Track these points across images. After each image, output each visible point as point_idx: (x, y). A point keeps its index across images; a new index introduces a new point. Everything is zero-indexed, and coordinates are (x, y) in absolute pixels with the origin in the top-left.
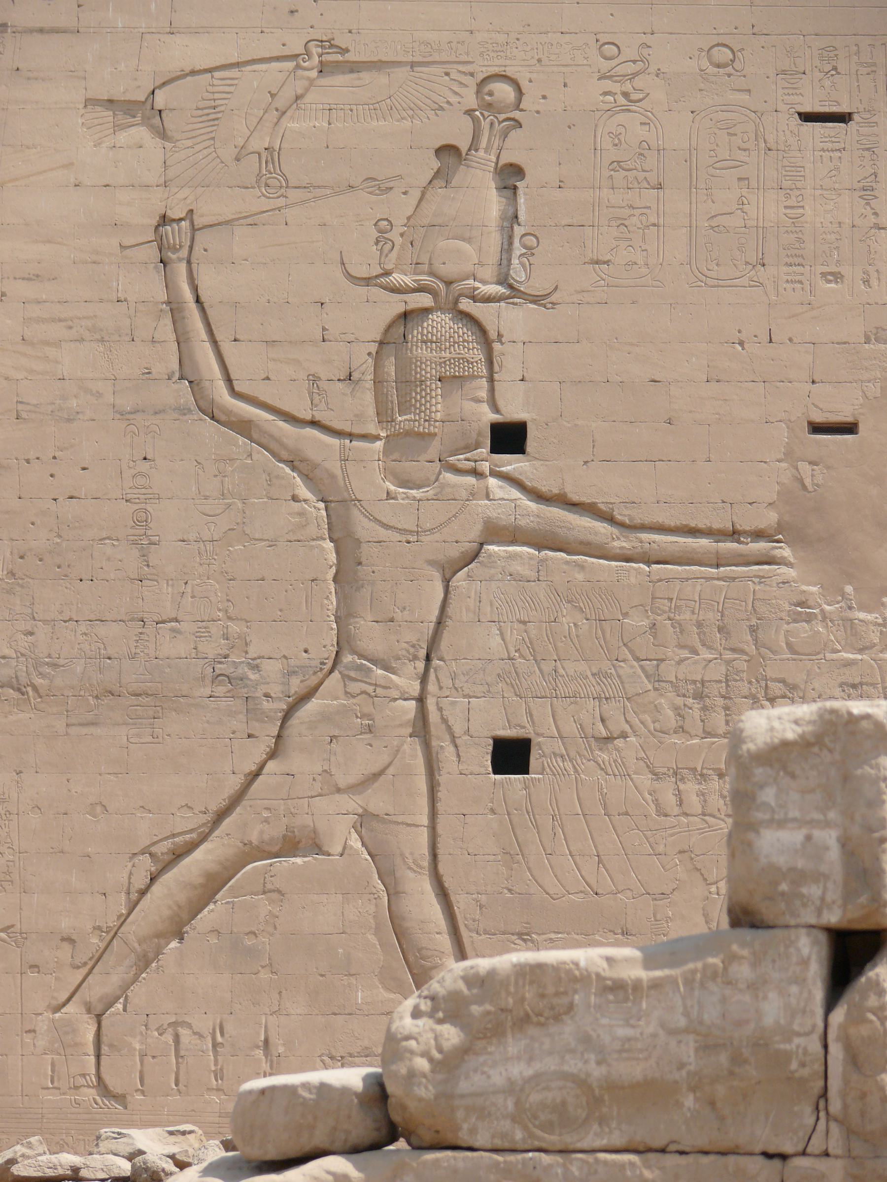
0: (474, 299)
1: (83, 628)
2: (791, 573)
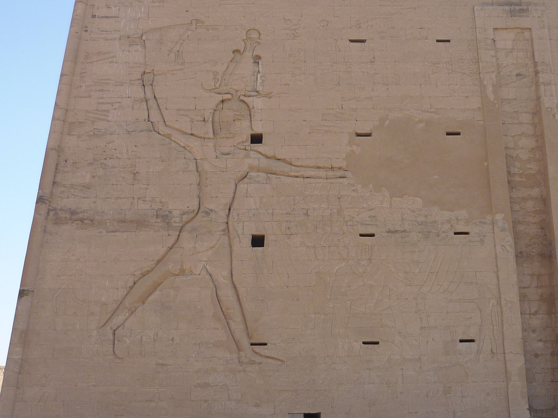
0: (245, 96)
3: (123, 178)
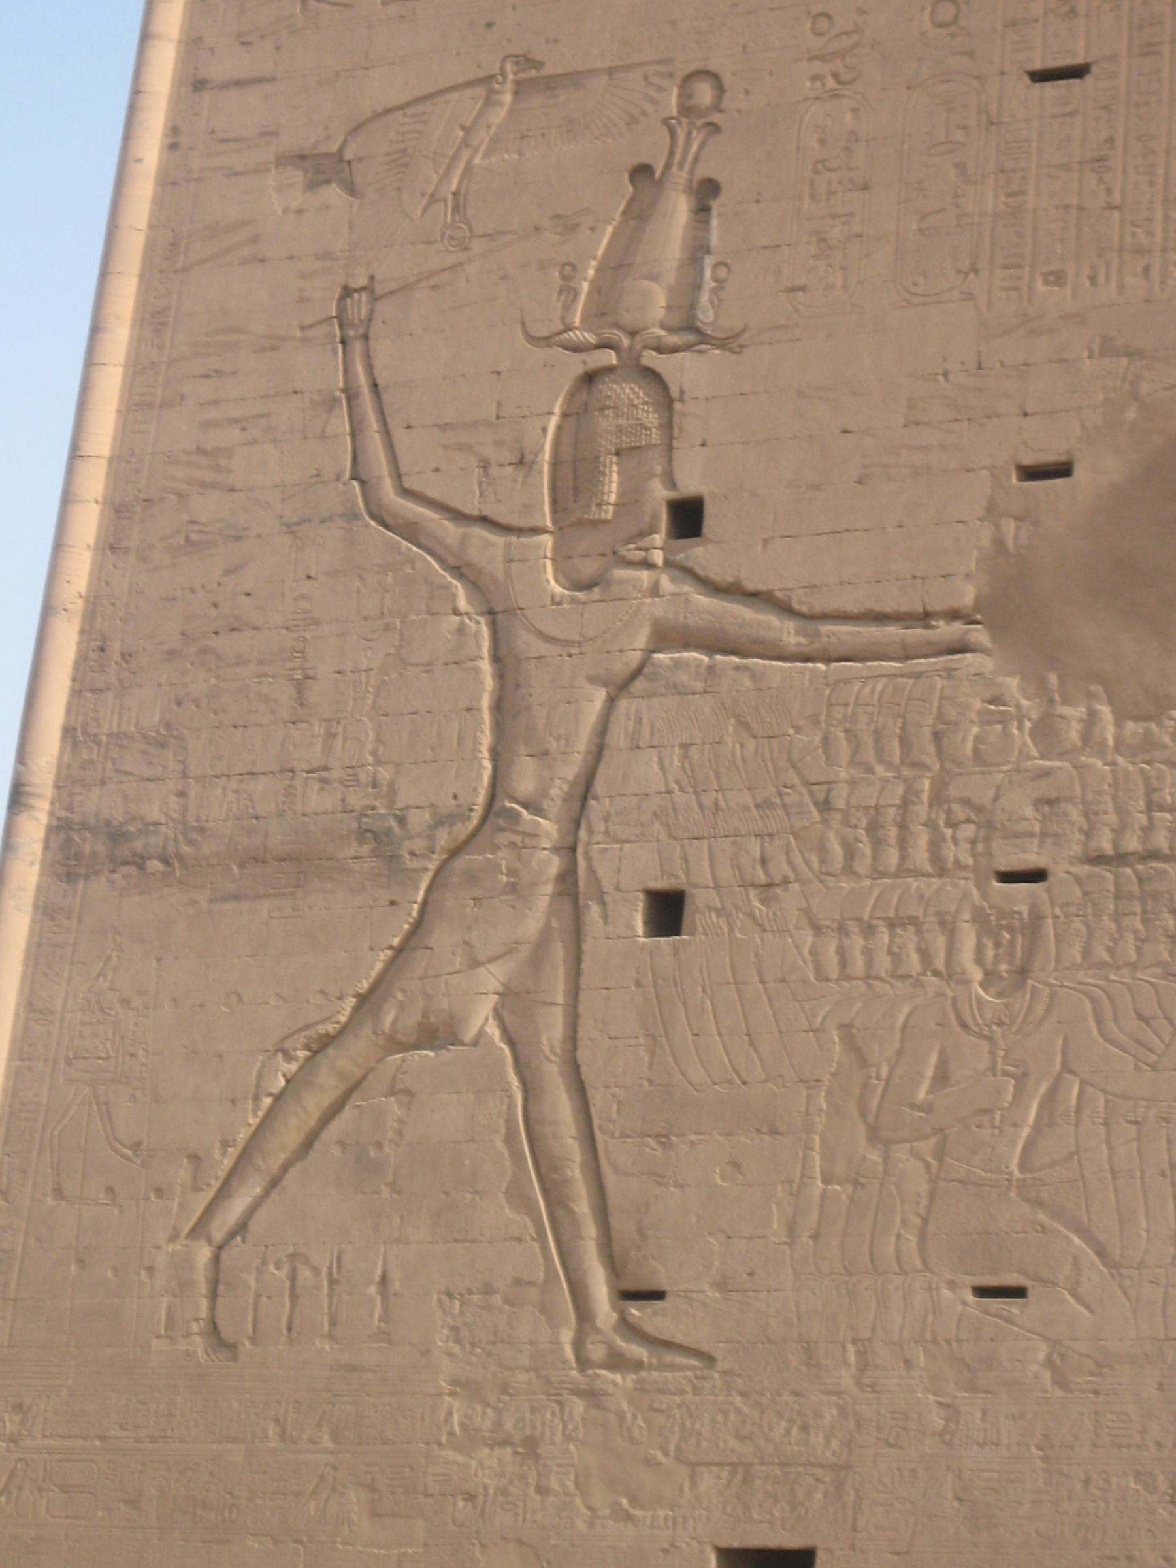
2: (987, 664)
3: (266, 699)
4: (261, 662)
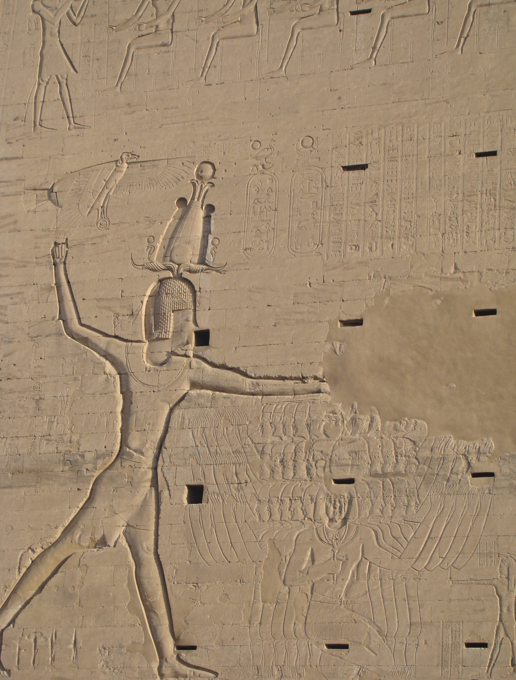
1: (9, 441)
3: (23, 407)
4: (20, 392)
